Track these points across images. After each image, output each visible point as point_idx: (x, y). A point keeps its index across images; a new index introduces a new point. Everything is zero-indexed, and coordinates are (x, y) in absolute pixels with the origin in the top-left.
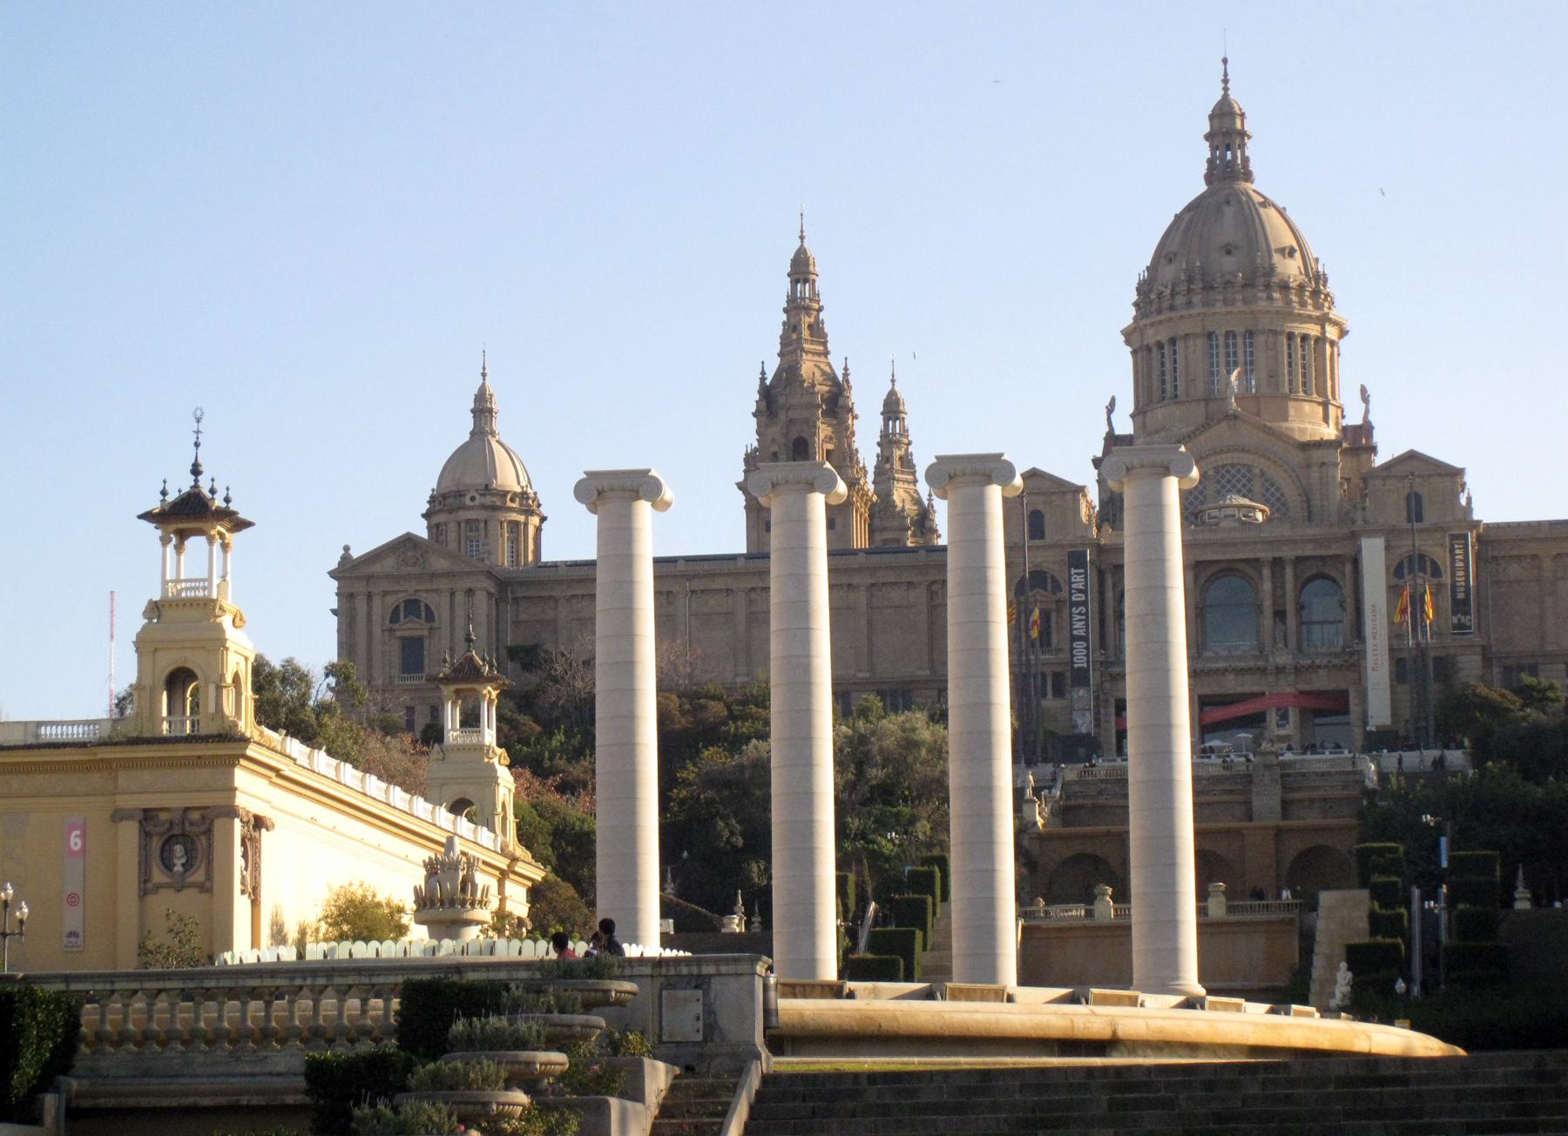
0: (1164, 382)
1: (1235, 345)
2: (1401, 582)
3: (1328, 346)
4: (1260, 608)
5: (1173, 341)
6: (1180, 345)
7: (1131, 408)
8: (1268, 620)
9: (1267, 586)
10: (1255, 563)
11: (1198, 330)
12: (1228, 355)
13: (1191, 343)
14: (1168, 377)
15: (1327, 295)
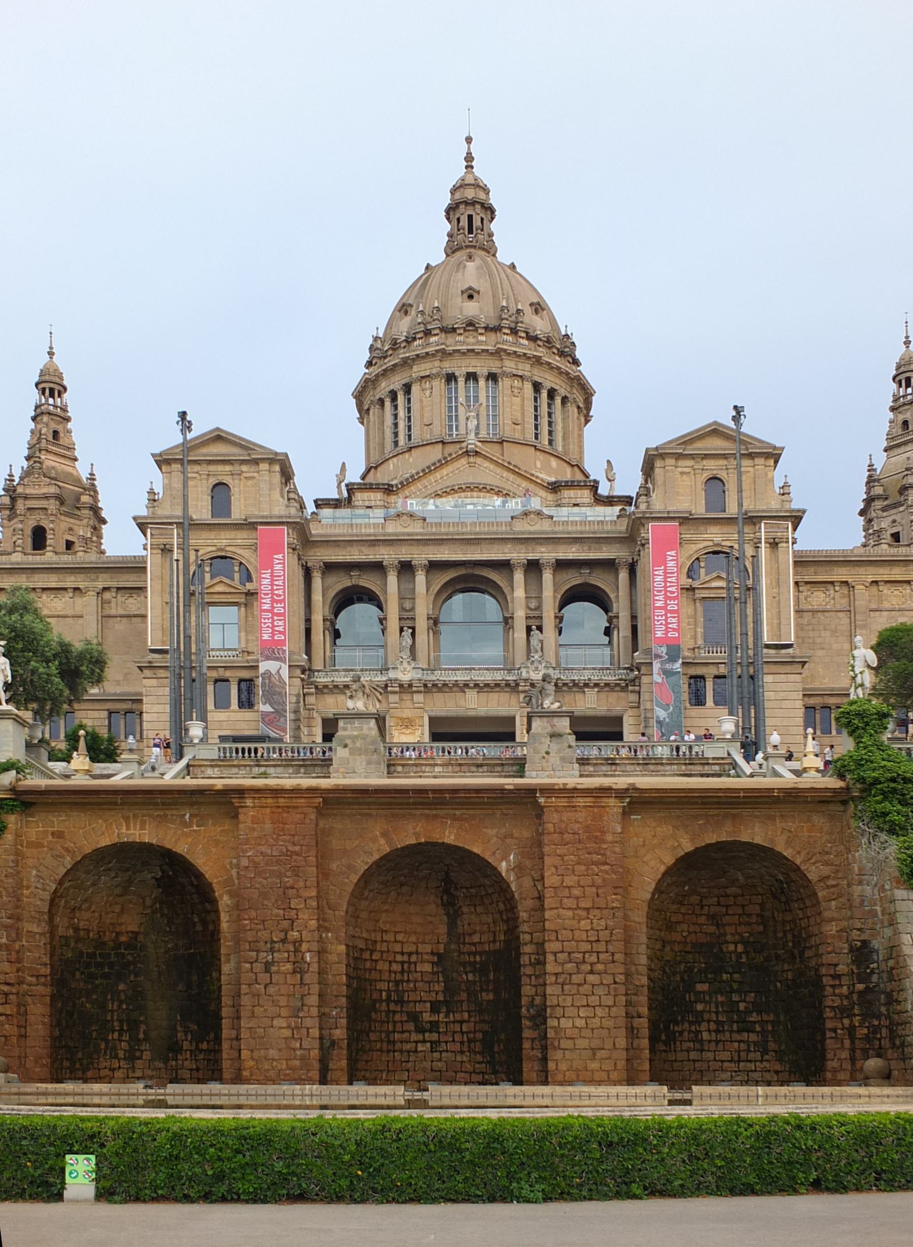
0: (396, 434)
1: (476, 391)
2: (696, 584)
3: (576, 410)
4: (508, 622)
5: (407, 388)
6: (415, 389)
7: (362, 469)
8: (520, 634)
9: (519, 593)
10: (505, 566)
11: (434, 371)
12: (468, 398)
13: (428, 385)
14: (402, 425)
15: (576, 362)
